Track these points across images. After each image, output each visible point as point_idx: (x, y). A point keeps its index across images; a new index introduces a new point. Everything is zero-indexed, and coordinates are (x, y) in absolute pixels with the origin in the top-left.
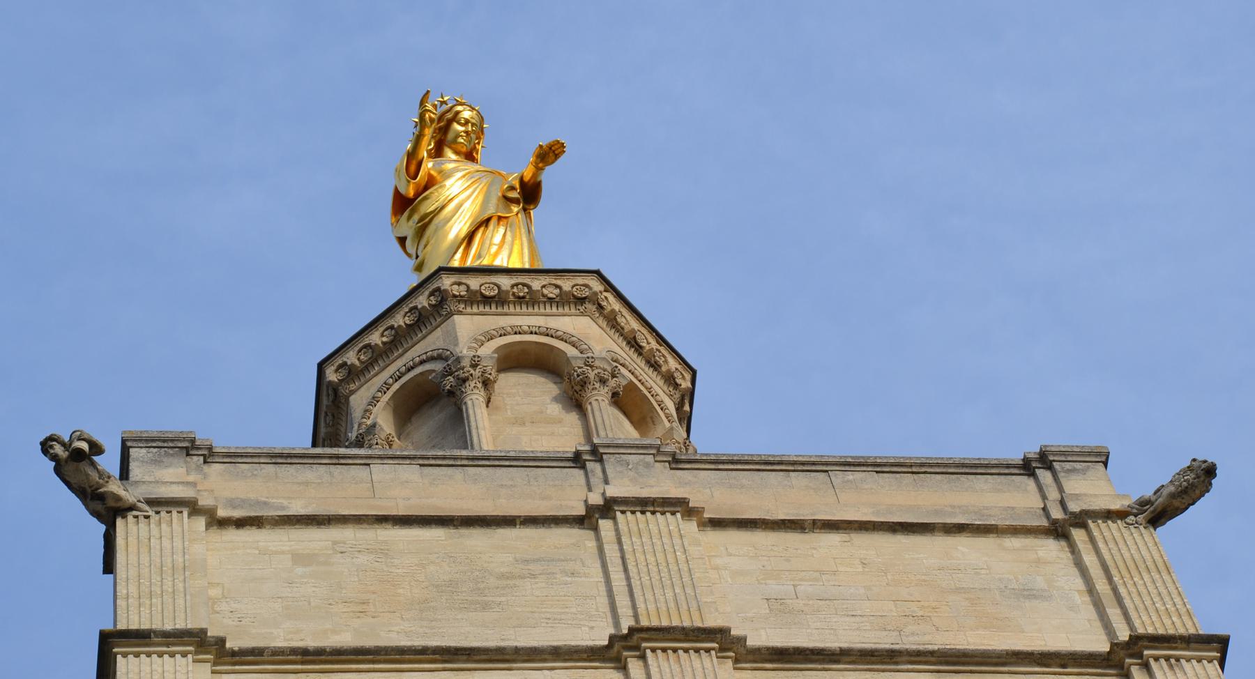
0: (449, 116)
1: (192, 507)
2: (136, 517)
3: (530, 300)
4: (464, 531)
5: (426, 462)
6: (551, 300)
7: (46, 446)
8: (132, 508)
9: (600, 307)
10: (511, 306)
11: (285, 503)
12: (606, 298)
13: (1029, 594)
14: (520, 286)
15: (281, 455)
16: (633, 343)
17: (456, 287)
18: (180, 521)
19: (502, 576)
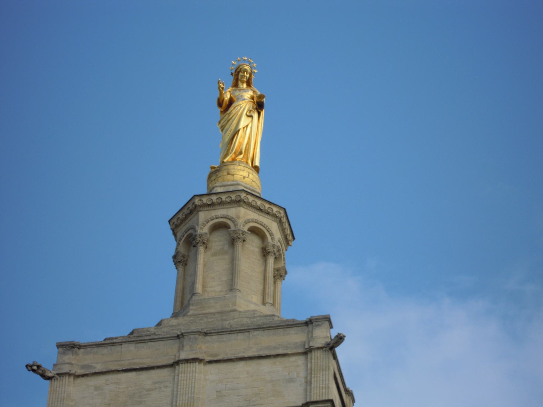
0: (239, 70)
1: (69, 374)
2: (54, 379)
3: (221, 204)
4: (141, 372)
5: (137, 342)
6: (229, 203)
7: (27, 366)
8: (53, 377)
9: (244, 202)
10: (217, 206)
11: (95, 365)
12: (247, 198)
13: (291, 380)
14: (219, 199)
15: (98, 345)
16: (259, 209)
17: (199, 201)
18: (66, 379)
19: (148, 390)
